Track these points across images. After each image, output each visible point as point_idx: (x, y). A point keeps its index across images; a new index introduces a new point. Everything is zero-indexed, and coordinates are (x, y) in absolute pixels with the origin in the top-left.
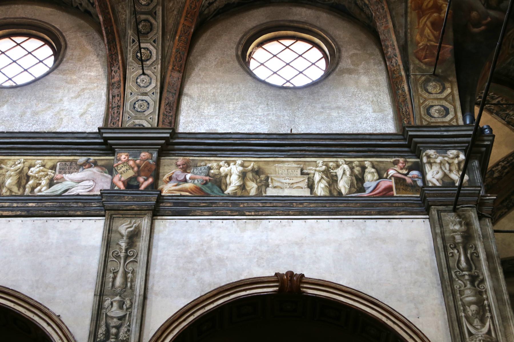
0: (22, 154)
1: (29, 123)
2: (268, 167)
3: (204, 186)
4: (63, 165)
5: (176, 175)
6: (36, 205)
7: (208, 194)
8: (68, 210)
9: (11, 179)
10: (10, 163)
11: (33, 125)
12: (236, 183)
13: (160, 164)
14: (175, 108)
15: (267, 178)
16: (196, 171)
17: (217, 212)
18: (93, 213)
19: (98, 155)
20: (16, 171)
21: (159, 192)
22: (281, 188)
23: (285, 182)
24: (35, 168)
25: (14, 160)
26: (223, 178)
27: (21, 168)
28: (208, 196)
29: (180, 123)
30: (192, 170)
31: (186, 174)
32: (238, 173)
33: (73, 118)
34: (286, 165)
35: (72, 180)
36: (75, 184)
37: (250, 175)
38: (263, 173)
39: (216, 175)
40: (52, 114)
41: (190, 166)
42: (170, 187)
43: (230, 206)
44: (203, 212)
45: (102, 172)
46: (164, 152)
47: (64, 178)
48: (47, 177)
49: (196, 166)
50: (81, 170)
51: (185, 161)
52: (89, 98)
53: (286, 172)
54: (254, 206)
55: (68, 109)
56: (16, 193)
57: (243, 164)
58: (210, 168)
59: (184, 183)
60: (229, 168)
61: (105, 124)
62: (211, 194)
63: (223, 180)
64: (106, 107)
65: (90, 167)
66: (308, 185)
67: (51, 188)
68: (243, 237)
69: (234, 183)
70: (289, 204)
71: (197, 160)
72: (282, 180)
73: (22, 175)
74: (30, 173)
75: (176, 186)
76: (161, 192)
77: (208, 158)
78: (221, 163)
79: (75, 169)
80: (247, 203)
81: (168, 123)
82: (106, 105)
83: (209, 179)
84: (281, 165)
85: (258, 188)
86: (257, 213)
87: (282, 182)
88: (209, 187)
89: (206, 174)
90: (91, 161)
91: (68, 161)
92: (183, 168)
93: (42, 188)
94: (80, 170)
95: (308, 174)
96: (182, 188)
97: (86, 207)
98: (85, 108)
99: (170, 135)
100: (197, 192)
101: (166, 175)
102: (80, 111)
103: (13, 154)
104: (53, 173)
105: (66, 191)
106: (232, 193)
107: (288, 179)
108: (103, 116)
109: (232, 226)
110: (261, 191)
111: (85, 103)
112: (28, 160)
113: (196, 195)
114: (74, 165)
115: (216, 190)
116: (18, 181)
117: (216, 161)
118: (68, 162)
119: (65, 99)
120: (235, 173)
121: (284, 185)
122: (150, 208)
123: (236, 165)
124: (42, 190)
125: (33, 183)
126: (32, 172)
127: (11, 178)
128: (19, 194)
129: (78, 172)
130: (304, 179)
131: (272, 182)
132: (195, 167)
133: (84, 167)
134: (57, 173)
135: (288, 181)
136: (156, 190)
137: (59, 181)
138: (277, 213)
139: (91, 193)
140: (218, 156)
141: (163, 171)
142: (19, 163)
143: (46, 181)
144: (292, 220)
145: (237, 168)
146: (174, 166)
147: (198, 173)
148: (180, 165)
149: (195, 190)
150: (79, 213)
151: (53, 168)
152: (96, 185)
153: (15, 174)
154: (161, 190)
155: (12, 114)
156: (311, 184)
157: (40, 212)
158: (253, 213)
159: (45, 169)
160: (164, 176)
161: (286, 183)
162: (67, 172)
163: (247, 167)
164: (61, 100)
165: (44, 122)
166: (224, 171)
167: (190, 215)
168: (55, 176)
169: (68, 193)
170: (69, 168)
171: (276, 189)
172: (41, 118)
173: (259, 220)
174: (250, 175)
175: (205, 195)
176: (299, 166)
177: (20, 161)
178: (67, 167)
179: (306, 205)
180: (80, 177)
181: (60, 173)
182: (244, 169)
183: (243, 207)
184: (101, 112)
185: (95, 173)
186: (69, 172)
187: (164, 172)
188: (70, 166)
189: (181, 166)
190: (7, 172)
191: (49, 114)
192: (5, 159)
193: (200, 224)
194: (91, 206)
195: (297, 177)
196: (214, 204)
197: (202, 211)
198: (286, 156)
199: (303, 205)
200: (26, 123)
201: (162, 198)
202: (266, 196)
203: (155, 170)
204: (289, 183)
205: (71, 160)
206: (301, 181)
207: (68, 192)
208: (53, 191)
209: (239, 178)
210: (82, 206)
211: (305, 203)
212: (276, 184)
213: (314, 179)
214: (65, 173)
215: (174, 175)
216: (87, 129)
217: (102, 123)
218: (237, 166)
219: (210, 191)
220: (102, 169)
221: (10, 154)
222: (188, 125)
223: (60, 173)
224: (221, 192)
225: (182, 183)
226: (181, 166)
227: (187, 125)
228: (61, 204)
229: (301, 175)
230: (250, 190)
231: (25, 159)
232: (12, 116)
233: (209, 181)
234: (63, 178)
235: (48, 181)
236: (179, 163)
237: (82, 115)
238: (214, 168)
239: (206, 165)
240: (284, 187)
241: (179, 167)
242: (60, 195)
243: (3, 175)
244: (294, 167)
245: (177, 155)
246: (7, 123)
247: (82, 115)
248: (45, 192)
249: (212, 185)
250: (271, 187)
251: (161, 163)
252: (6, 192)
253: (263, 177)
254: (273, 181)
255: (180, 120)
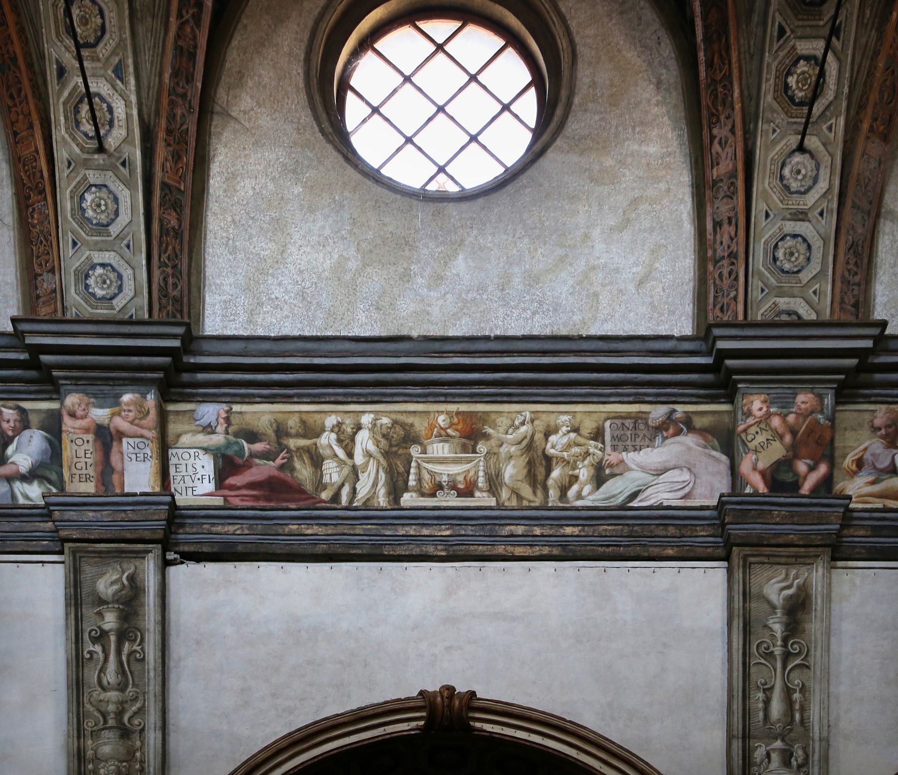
0: (526, 399)
1: (524, 310)
4: (618, 429)
6: (580, 531)
8: (647, 543)
9: (514, 466)
10: (503, 422)
11: (534, 313)
14: (866, 260)
18: (699, 551)
19: (694, 400)
20: (520, 443)
24: (558, 436)
25: (510, 414)
27: (529, 437)
33: (621, 291)
35: (643, 469)
36: (651, 478)
40: (571, 282)
45: (705, 447)
47: (626, 461)
48: (588, 458)
50: (658, 440)
52: (652, 230)
55: (605, 266)
56: (530, 501)
61: (698, 309)
64: (695, 258)
65: (678, 433)
67: (601, 490)
73: (536, 456)
74: (551, 451)
79: (647, 439)
81: (852, 306)
82: (695, 251)
90: (678, 415)
91: (628, 416)
93: (581, 490)
94: (657, 442)
97: (684, 537)
98: (647, 262)
102: (634, 270)
103: (505, 399)
104: (600, 450)
105: (634, 496)
108: (692, 284)
111: (643, 245)
112: (540, 415)
114: (642, 427)
116: (529, 471)
118: (629, 421)
119: (596, 233)
124: (585, 491)
125: (561, 475)
126: (553, 447)
127: (512, 462)
128: (537, 504)
129: (654, 447)
133: (665, 434)
134: (608, 449)
137: (616, 471)
139: (689, 503)
142: (523, 423)
143: (588, 471)
150: (670, 552)
151: (598, 435)
152: (698, 481)
153: (519, 453)
155: (480, 283)
157: (588, 548)
159: (581, 440)
162: (630, 448)
164: (587, 236)
165: (557, 304)
168: (605, 459)
169: (639, 501)
170: (633, 437)
172: (549, 293)
177: (523, 418)
178: (629, 433)
180: (660, 460)
181: (614, 448)
184: (685, 272)
185: (689, 449)
186: (633, 446)
188: (634, 432)
190: (501, 445)
191: (565, 282)
192: (491, 412)
194: (695, 534)
200: (516, 307)
205: (632, 415)
207: (639, 499)
208: (607, 495)
210: (678, 535)
214: (626, 450)
216: (658, 325)
217: (691, 305)
220: (706, 440)
221: (499, 399)
223: (614, 448)
228: (631, 528)
231: (533, 412)
232: (482, 288)
234: (622, 461)
235: (592, 471)
237: (641, 283)
242: (622, 507)
243: (495, 454)
246: (474, 309)
247: (641, 283)
248: (591, 497)
252: (509, 499)
255: (875, 296)
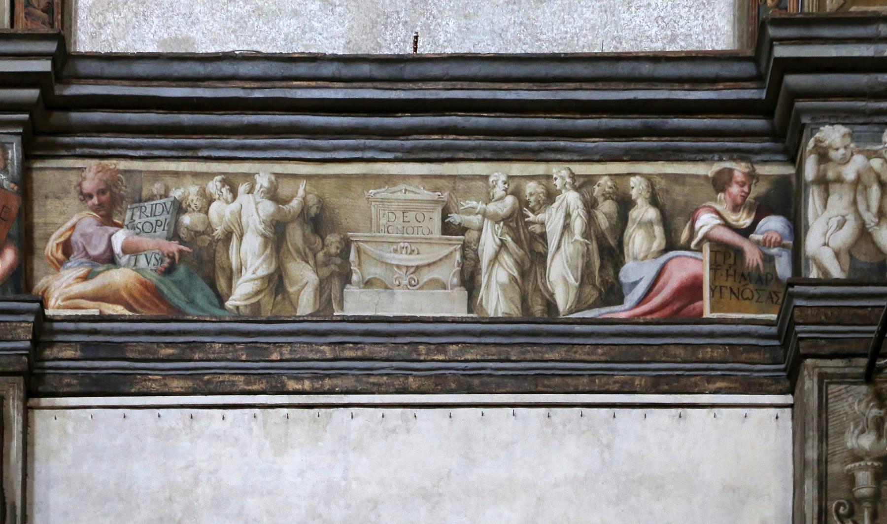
2: (348, 200)
3: (167, 280)
5: (82, 235)
7: (179, 310)
12: (256, 270)
13: (31, 188)
15: (347, 244)
16: (140, 218)
17: (209, 382)
21: (36, 306)
22: (386, 288)
23: (396, 262)
26: (220, 247)
28: (181, 317)
29: (80, 12)
30: (129, 214)
31: (111, 229)
32: (261, 227)
34: (400, 193)
37: (296, 235)
38: (335, 227)
39: (198, 234)
41: (123, 198)
42: (70, 285)
43: (244, 357)
44: (168, 381)
46: (41, 139)
49: (137, 198)
51: (105, 178)
53: (399, 223)
54: (310, 356)
57: (276, 189)
58: (180, 208)
59: (108, 269)
60: (234, 206)
62: (188, 309)
63: (220, 257)
66: (462, 272)
68: (280, 471)
69: (253, 268)
70: (406, 347)
71: (141, 172)
72: (388, 255)
75: (85, 278)
76: (43, 302)
77: (172, 166)
78: (213, 186)
80: (289, 343)
83: (181, 252)
84: (384, 193)
85: (322, 288)
86: (317, 385)
87: (387, 264)
88: (178, 284)
89: (168, 231)
92: (101, 204)
95: (462, 230)
96: (104, 287)
99: (54, 65)
100: (148, 304)
101: (53, 237)
106: (246, 306)
107: (404, 251)
109: (251, 430)
110: (329, 301)
113: (146, 313)
115: (202, 295)
117: (196, 175)
120: (252, 226)
121: (394, 273)
122: (18, 368)
123: (255, 192)
130: (452, 248)
131: (360, 265)
132: (135, 202)
135: (404, 259)
136: (26, 297)
138: (374, 384)
140: (201, 154)
141: (42, 220)
144: (414, 410)
145: (257, 204)
146: (72, 201)
147: (147, 228)
148: (91, 196)
149: (142, 294)
154: (43, 296)
156: (470, 270)
158: (307, 385)
160: (47, 238)
161: (398, 266)
163: (286, 202)
166: (221, 218)
167: (133, 390)
171: (370, 291)
173: (323, 410)
174: (296, 235)
175: (170, 317)
176: (435, 196)
179: (455, 352)
182: (279, 210)
183: (281, 361)
187: (46, 224)
189: (95, 200)
193: (160, 424)
195: (429, 242)
196: (197, 347)
197: (164, 376)
198: (399, 155)
199: (445, 352)
201: (47, 325)
202: (344, 320)
203: (19, 214)
204: (407, 267)
206: (441, 260)
209: (266, 247)
211: (452, 344)
212: (373, 271)
213: (480, 248)
215: (76, 238)
218: (259, 200)
219: (183, 297)
222: (105, 18)
224: (216, 302)
225: (101, 269)
226: (95, 200)
227: (100, 19)
229: (442, 234)
230: (299, 292)
233: (180, 259)
236: (88, 186)
238: (193, 206)
239: (166, 195)
240: (392, 285)
241: (90, 203)
244: (422, 201)
245: (78, 151)
249: (190, 275)
250: (358, 284)
251: (35, 185)
253: (333, 239)
254: (363, 257)
